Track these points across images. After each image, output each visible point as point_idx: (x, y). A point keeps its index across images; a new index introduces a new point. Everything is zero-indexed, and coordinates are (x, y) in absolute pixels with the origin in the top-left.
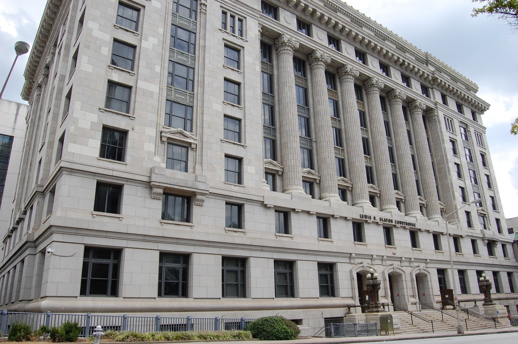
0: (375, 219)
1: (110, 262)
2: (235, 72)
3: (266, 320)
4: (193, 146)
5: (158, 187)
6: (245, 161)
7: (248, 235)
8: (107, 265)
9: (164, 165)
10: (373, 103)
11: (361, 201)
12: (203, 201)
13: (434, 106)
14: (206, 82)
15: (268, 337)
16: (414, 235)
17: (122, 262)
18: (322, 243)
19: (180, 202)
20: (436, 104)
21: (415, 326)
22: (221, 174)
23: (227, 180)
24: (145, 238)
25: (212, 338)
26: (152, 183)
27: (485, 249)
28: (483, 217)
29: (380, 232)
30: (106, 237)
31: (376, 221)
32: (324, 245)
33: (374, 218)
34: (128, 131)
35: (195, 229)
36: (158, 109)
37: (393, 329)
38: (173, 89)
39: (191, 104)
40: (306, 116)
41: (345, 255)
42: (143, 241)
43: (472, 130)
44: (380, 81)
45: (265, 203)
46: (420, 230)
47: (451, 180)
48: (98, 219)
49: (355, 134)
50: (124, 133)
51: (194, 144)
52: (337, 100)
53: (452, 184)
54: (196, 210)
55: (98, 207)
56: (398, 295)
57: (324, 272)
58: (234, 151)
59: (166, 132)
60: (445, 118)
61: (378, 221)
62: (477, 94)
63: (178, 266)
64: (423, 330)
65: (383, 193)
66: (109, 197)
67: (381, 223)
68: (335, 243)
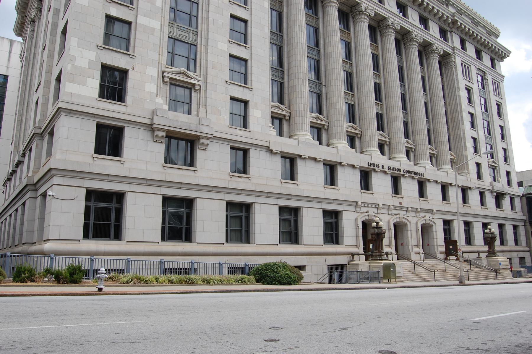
0: (383, 168)
1: (113, 206)
2: (242, 8)
3: (270, 265)
4: (197, 87)
5: (161, 130)
6: (251, 105)
7: (253, 181)
8: (110, 209)
9: (166, 107)
10: (388, 46)
11: (369, 149)
12: (207, 145)
13: (452, 51)
14: (211, 19)
15: (272, 282)
16: (422, 185)
17: (125, 206)
18: (328, 190)
19: (183, 146)
20: (454, 49)
21: (417, 275)
22: (226, 117)
23: (232, 124)
24: (148, 182)
25: (215, 282)
26: (154, 126)
27: (494, 201)
28: (493, 169)
29: (388, 181)
30: (108, 181)
31: (384, 170)
32: (330, 193)
33: (383, 166)
34: (128, 70)
35: (198, 174)
36: (160, 47)
37: (395, 278)
38: (175, 26)
39: (194, 43)
40: (316, 57)
41: (351, 203)
42: (146, 185)
43: (489, 78)
44: (396, 22)
45: (271, 148)
46: (428, 180)
47: (464, 130)
48: (99, 162)
49: (367, 78)
50: (124, 73)
51: (198, 85)
52: (349, 41)
53: (464, 134)
54: (199, 154)
55: (99, 149)
56: (402, 244)
57: (329, 220)
58: (240, 93)
59: (168, 72)
60: (462, 64)
61: (386, 169)
62: (499, 40)
63: (182, 211)
64: (425, 279)
65: (393, 141)
66: (109, 140)
67: (389, 172)
68: (341, 191)
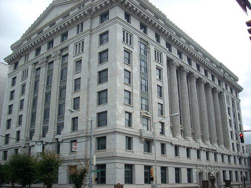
20: (223, 89)
29: (185, 151)
30: (130, 160)
43: (235, 101)
62: (238, 83)
